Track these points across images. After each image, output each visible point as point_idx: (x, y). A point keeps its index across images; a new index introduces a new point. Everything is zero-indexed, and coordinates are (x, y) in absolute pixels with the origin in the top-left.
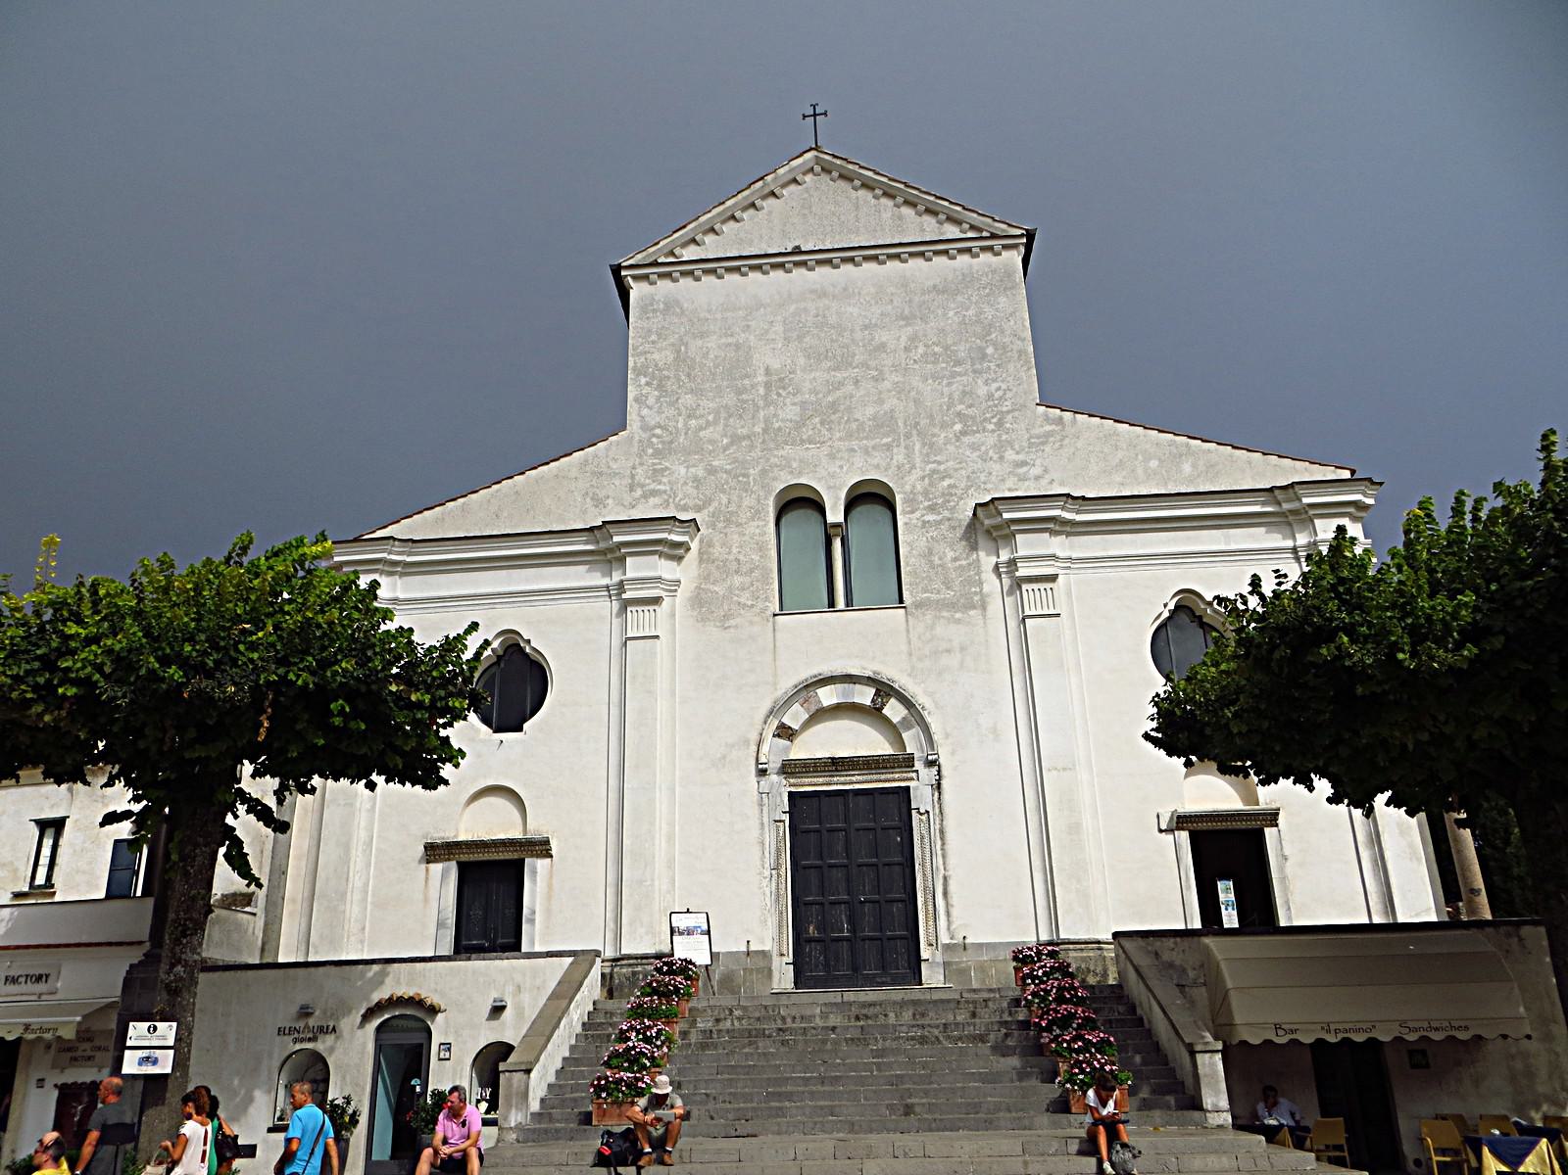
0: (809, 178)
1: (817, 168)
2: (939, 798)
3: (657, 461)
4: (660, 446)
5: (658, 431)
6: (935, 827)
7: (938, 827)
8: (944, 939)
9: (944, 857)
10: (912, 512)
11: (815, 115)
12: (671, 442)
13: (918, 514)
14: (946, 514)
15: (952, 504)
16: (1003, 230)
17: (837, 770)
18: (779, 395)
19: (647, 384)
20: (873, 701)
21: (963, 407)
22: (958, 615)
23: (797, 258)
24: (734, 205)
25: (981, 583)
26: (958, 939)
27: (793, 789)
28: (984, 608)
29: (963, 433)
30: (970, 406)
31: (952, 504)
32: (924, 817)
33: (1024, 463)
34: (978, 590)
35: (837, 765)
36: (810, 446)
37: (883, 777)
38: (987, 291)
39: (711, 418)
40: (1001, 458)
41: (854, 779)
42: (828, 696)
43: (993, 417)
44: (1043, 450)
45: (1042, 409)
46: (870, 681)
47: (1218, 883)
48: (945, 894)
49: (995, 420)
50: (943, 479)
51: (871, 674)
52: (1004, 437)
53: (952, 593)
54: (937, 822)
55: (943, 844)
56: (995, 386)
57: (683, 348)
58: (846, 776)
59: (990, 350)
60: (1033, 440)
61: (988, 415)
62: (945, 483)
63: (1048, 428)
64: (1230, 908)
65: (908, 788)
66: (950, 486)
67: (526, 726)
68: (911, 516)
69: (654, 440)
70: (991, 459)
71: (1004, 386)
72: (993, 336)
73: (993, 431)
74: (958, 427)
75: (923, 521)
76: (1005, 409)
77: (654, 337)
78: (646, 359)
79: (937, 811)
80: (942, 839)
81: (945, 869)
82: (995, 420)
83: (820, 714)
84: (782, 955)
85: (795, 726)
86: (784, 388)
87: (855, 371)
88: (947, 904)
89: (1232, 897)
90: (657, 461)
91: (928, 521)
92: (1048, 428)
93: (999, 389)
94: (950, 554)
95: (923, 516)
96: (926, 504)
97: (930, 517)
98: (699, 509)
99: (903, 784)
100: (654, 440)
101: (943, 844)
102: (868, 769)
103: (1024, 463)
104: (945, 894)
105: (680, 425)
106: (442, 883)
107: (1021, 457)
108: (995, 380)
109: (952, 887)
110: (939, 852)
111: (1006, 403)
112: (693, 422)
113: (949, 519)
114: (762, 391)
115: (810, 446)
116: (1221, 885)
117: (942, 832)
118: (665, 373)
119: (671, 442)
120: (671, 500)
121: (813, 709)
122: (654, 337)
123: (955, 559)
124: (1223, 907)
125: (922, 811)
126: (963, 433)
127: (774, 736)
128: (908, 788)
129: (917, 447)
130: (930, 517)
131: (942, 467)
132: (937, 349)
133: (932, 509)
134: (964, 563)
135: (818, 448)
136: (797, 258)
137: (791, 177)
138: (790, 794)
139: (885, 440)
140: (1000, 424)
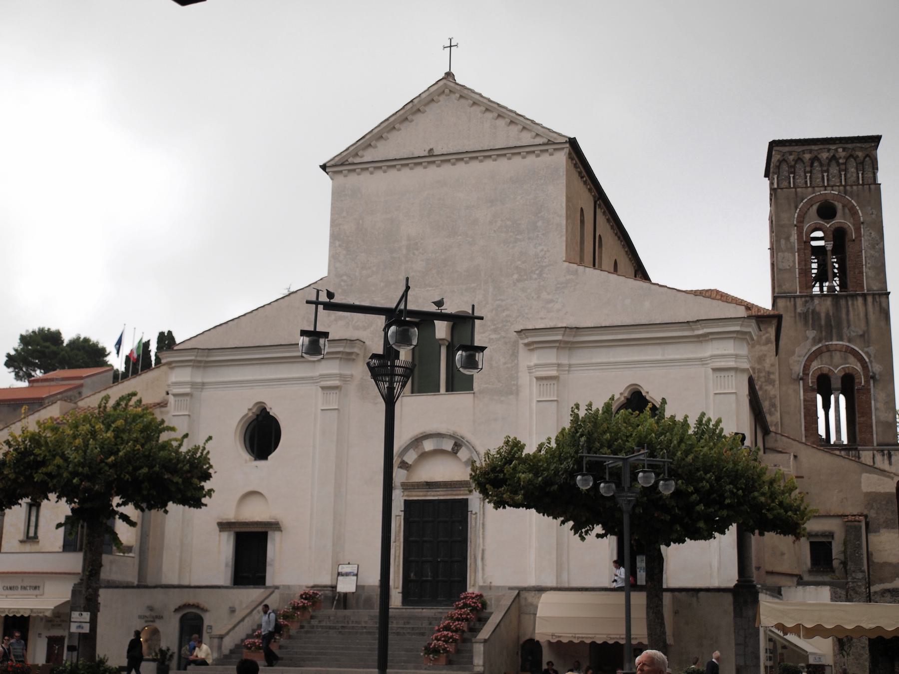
0: (442, 98)
1: (447, 91)
2: (483, 506)
3: (343, 297)
4: (346, 287)
5: (345, 278)
6: (479, 522)
7: (481, 522)
8: (481, 584)
9: (483, 538)
10: (484, 333)
11: (451, 46)
12: (352, 285)
13: (487, 334)
14: (503, 334)
15: (507, 327)
16: (555, 139)
17: (429, 488)
18: (414, 254)
19: (340, 246)
20: (453, 449)
21: (519, 262)
22: (503, 398)
23: (431, 158)
24: (394, 121)
25: (517, 378)
26: (487, 584)
27: (407, 498)
28: (517, 394)
29: (519, 281)
30: (524, 262)
31: (507, 327)
32: (474, 516)
33: (551, 301)
34: (515, 383)
35: (430, 485)
36: (430, 289)
37: (455, 493)
38: (542, 181)
39: (374, 269)
40: (539, 297)
41: (438, 493)
42: (428, 446)
43: (536, 270)
44: (564, 293)
45: (567, 264)
46: (451, 437)
47: (637, 557)
48: (483, 559)
49: (537, 272)
50: (504, 311)
51: (451, 432)
52: (542, 283)
53: (501, 385)
54: (481, 519)
55: (483, 531)
56: (540, 248)
57: (361, 221)
58: (436, 491)
59: (540, 224)
60: (558, 286)
61: (534, 269)
62: (504, 314)
63: (568, 277)
64: (642, 571)
65: (467, 499)
66: (507, 316)
67: (269, 457)
68: (483, 335)
69: (342, 283)
70: (533, 297)
71: (545, 249)
72: (542, 214)
73: (536, 279)
74: (516, 276)
75: (490, 339)
76: (544, 264)
77: (344, 214)
78: (339, 229)
79: (482, 512)
80: (483, 528)
81: (484, 545)
82: (537, 272)
83: (424, 456)
84: (397, 588)
85: (410, 462)
86: (417, 250)
87: (460, 237)
88: (483, 565)
89: (644, 565)
90: (343, 297)
91: (492, 339)
92: (568, 277)
93: (542, 250)
94: (502, 360)
95: (489, 335)
96: (492, 327)
97: (494, 336)
98: (365, 328)
99: (465, 497)
100: (342, 283)
101: (483, 531)
102: (446, 488)
103: (551, 301)
104: (483, 559)
105: (357, 274)
106: (225, 547)
107: (550, 297)
108: (540, 244)
109: (487, 556)
110: (481, 536)
111: (545, 260)
112: (364, 272)
113: (504, 337)
114: (404, 251)
115: (430, 289)
116: (639, 558)
117: (483, 524)
118: (350, 238)
119: (352, 285)
120: (350, 323)
121: (420, 452)
122: (344, 214)
123: (505, 363)
124: (638, 570)
125: (474, 512)
126: (519, 281)
127: (398, 467)
128: (467, 499)
129: (491, 290)
130: (494, 336)
131: (504, 303)
132: (509, 223)
133: (495, 331)
134: (509, 365)
135: (434, 290)
136: (431, 158)
137: (430, 98)
138: (405, 501)
139: (473, 285)
140: (540, 274)
